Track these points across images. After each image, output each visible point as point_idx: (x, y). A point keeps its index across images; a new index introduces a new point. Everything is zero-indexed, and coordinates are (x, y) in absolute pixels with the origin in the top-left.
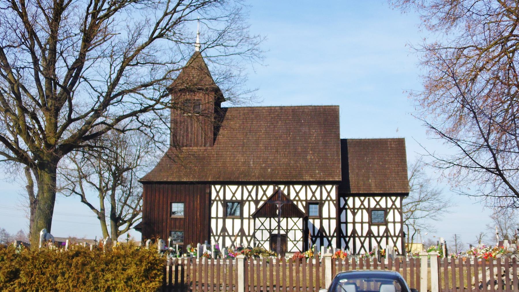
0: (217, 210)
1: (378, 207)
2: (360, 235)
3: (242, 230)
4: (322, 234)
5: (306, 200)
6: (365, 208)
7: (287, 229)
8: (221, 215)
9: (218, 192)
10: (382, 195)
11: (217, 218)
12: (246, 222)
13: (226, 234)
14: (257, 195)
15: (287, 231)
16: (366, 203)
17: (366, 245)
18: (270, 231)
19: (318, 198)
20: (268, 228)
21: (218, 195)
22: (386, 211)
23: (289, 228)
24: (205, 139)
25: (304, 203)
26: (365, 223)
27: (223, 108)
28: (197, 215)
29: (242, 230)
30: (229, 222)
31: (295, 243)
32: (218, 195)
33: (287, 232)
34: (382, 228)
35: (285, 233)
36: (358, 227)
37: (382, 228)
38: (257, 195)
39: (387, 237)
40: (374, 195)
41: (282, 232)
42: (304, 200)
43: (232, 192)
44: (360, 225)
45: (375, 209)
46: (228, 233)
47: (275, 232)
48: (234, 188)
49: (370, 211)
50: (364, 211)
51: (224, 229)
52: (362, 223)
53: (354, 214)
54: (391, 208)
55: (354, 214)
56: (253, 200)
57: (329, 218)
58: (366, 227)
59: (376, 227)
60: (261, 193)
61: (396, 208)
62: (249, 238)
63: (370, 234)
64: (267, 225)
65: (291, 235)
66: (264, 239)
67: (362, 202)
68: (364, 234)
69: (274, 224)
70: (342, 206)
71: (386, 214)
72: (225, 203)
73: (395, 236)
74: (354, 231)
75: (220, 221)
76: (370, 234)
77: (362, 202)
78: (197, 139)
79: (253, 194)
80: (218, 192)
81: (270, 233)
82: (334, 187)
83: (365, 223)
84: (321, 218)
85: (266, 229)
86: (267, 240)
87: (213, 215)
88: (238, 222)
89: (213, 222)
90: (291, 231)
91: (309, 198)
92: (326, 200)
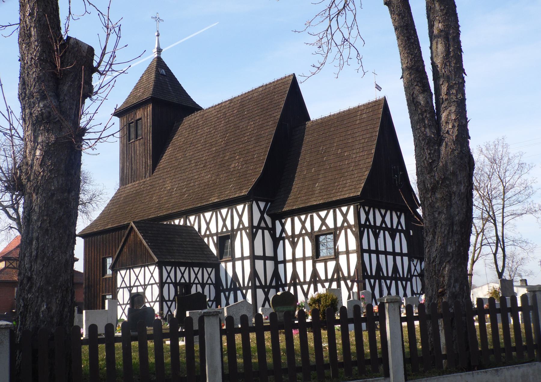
2: (302, 280)
4: (295, 281)
15: (145, 286)
18: (130, 288)
22: (335, 233)
25: (215, 238)
26: (308, 258)
33: (145, 289)
34: (331, 265)
35: (143, 291)
39: (338, 281)
41: (140, 290)
44: (302, 262)
47: (134, 290)
52: (304, 259)
55: (294, 245)
57: (242, 259)
68: (308, 279)
70: (278, 235)
74: (295, 275)
81: (130, 291)
83: (308, 258)
84: (233, 260)
92: (239, 229)
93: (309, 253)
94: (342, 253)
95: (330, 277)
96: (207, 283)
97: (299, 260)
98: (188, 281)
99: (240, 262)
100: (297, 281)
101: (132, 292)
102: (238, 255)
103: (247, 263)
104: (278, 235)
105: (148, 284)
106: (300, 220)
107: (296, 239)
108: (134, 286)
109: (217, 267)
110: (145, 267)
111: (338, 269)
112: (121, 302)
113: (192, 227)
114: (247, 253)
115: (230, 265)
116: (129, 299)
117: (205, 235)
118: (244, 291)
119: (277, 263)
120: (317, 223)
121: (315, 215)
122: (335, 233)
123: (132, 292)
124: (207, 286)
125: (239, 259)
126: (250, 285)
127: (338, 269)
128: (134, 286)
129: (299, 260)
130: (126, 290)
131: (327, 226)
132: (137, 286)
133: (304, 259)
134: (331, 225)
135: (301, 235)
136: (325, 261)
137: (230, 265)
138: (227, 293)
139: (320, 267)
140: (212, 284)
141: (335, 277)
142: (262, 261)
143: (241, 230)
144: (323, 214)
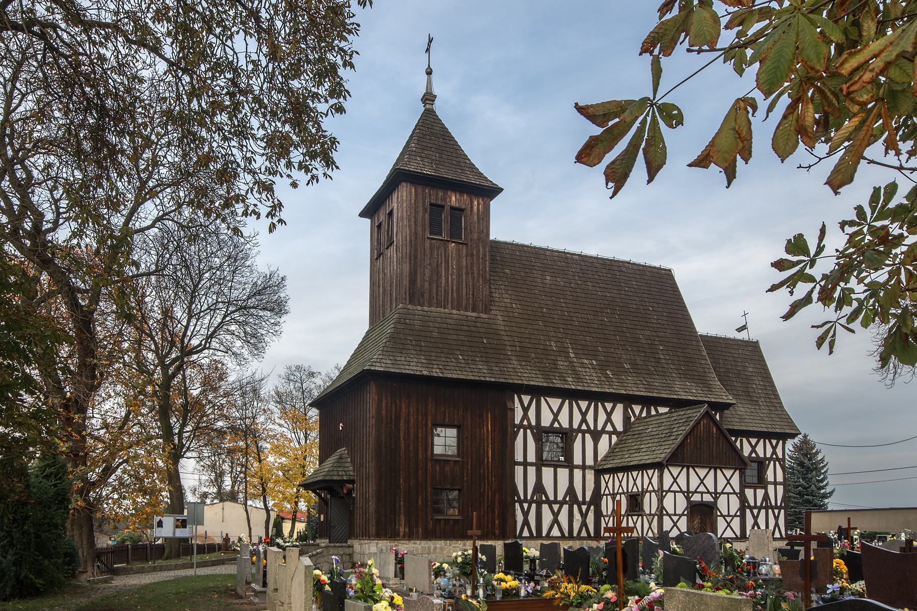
0: (524, 447)
1: (754, 455)
3: (571, 490)
7: (716, 492)
8: (532, 458)
9: (526, 410)
10: (760, 435)
11: (525, 464)
12: (578, 473)
13: (544, 498)
14: (596, 420)
15: (716, 495)
18: (688, 494)
20: (684, 489)
21: (525, 416)
23: (719, 490)
24: (473, 295)
27: (497, 244)
28: (488, 457)
29: (571, 490)
30: (547, 472)
31: (729, 519)
32: (525, 416)
33: (716, 499)
37: (760, 493)
38: (596, 420)
41: (708, 498)
43: (551, 412)
46: (547, 496)
47: (696, 498)
48: (555, 403)
51: (539, 488)
56: (588, 430)
60: (602, 417)
62: (526, 505)
64: (682, 480)
65: (722, 503)
66: (679, 511)
69: (694, 482)
72: (540, 433)
75: (532, 471)
78: (458, 294)
79: (590, 417)
80: (526, 410)
81: (688, 498)
85: (681, 491)
86: (683, 514)
87: (519, 457)
88: (563, 473)
89: (519, 470)
111: (766, 497)
127: (766, 497)
128: (696, 492)
130: (680, 496)
131: (756, 453)
134: (761, 455)
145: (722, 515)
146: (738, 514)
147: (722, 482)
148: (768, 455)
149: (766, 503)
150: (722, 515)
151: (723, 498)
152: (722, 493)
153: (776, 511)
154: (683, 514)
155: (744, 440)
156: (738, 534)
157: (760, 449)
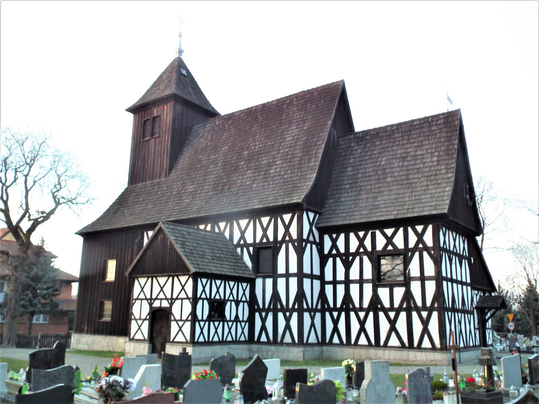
1: (390, 248)
2: (357, 305)
5: (254, 245)
6: (366, 252)
7: (172, 299)
15: (172, 301)
16: (368, 243)
17: (369, 326)
18: (151, 301)
19: (400, 245)
22: (406, 255)
25: (251, 249)
26: (367, 281)
33: (171, 304)
34: (399, 292)
35: (168, 305)
36: (354, 289)
40: (382, 225)
41: (165, 304)
42: (251, 245)
44: (358, 285)
45: (385, 253)
47: (156, 304)
49: (376, 258)
50: (365, 258)
52: (361, 282)
53: (348, 265)
54: (416, 248)
55: (348, 265)
57: (287, 275)
58: (368, 288)
59: (387, 290)
61: (426, 248)
63: (376, 304)
67: (361, 241)
68: (366, 305)
70: (326, 252)
71: (406, 263)
73: (424, 308)
76: (376, 304)
77: (361, 241)
81: (151, 304)
82: (430, 227)
83: (367, 281)
84: (275, 276)
86: (146, 319)
90: (177, 301)
91: (258, 241)
93: (368, 274)
94: (415, 279)
95: (396, 305)
96: (241, 301)
97: (354, 282)
98: (222, 298)
99: (284, 279)
100: (351, 306)
101: (154, 305)
102: (281, 269)
103: (293, 281)
104: (326, 252)
105: (177, 298)
106: (357, 236)
107: (351, 258)
108: (156, 299)
109: (252, 282)
110: (169, 276)
111: (408, 296)
112: (137, 317)
113: (222, 234)
114: (293, 269)
115: (269, 282)
116: (149, 314)
117: (238, 245)
118: (288, 314)
119: (323, 283)
120: (381, 242)
121: (378, 233)
122: (406, 255)
123: (154, 305)
124: (241, 304)
125: (282, 276)
126: (296, 307)
127: (408, 296)
128: (156, 299)
129: (354, 282)
130: (145, 303)
132: (161, 299)
133: (361, 282)
135: (357, 253)
136: (391, 287)
137: (269, 282)
138: (264, 314)
139: (383, 293)
140: (246, 301)
141: (405, 306)
142: (310, 280)
143: (287, 243)
144: (389, 232)
145: (175, 320)
146: (190, 318)
147: (177, 287)
148: (411, 245)
149: (323, 306)
150: (175, 320)
151: (178, 303)
152: (177, 298)
153: (335, 314)
154: (146, 319)
155: (378, 233)
156: (188, 338)
157: (399, 241)
